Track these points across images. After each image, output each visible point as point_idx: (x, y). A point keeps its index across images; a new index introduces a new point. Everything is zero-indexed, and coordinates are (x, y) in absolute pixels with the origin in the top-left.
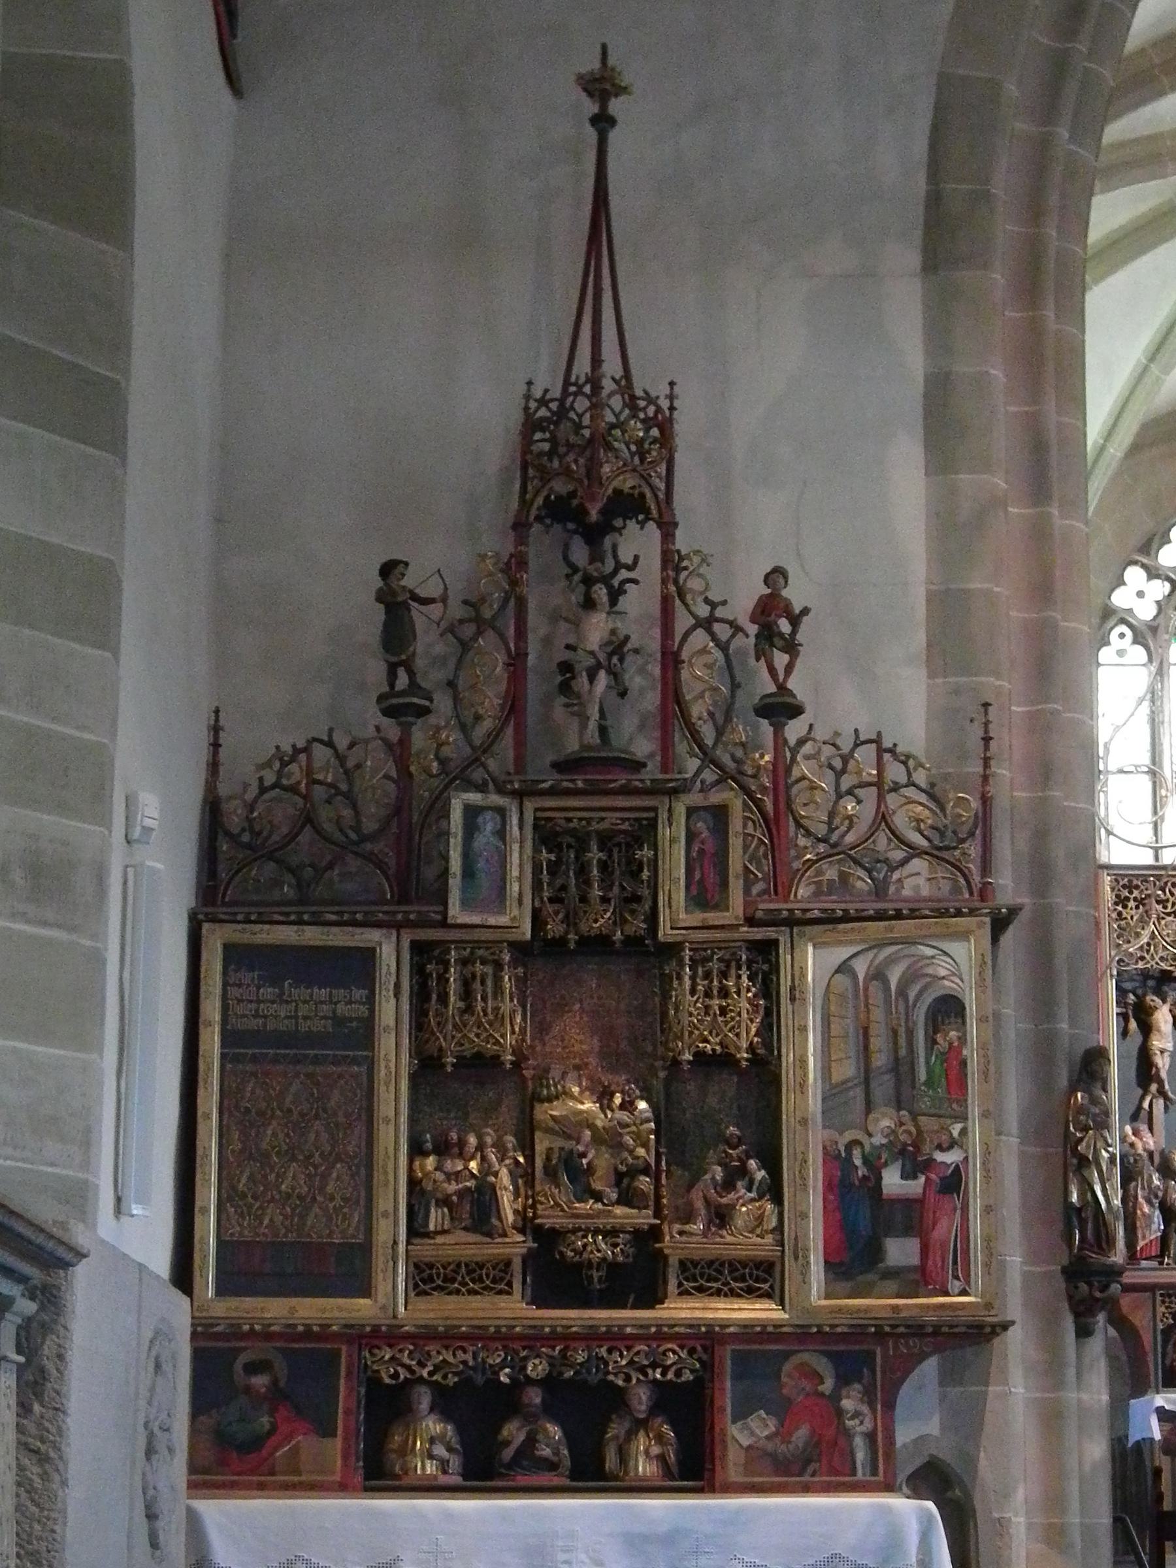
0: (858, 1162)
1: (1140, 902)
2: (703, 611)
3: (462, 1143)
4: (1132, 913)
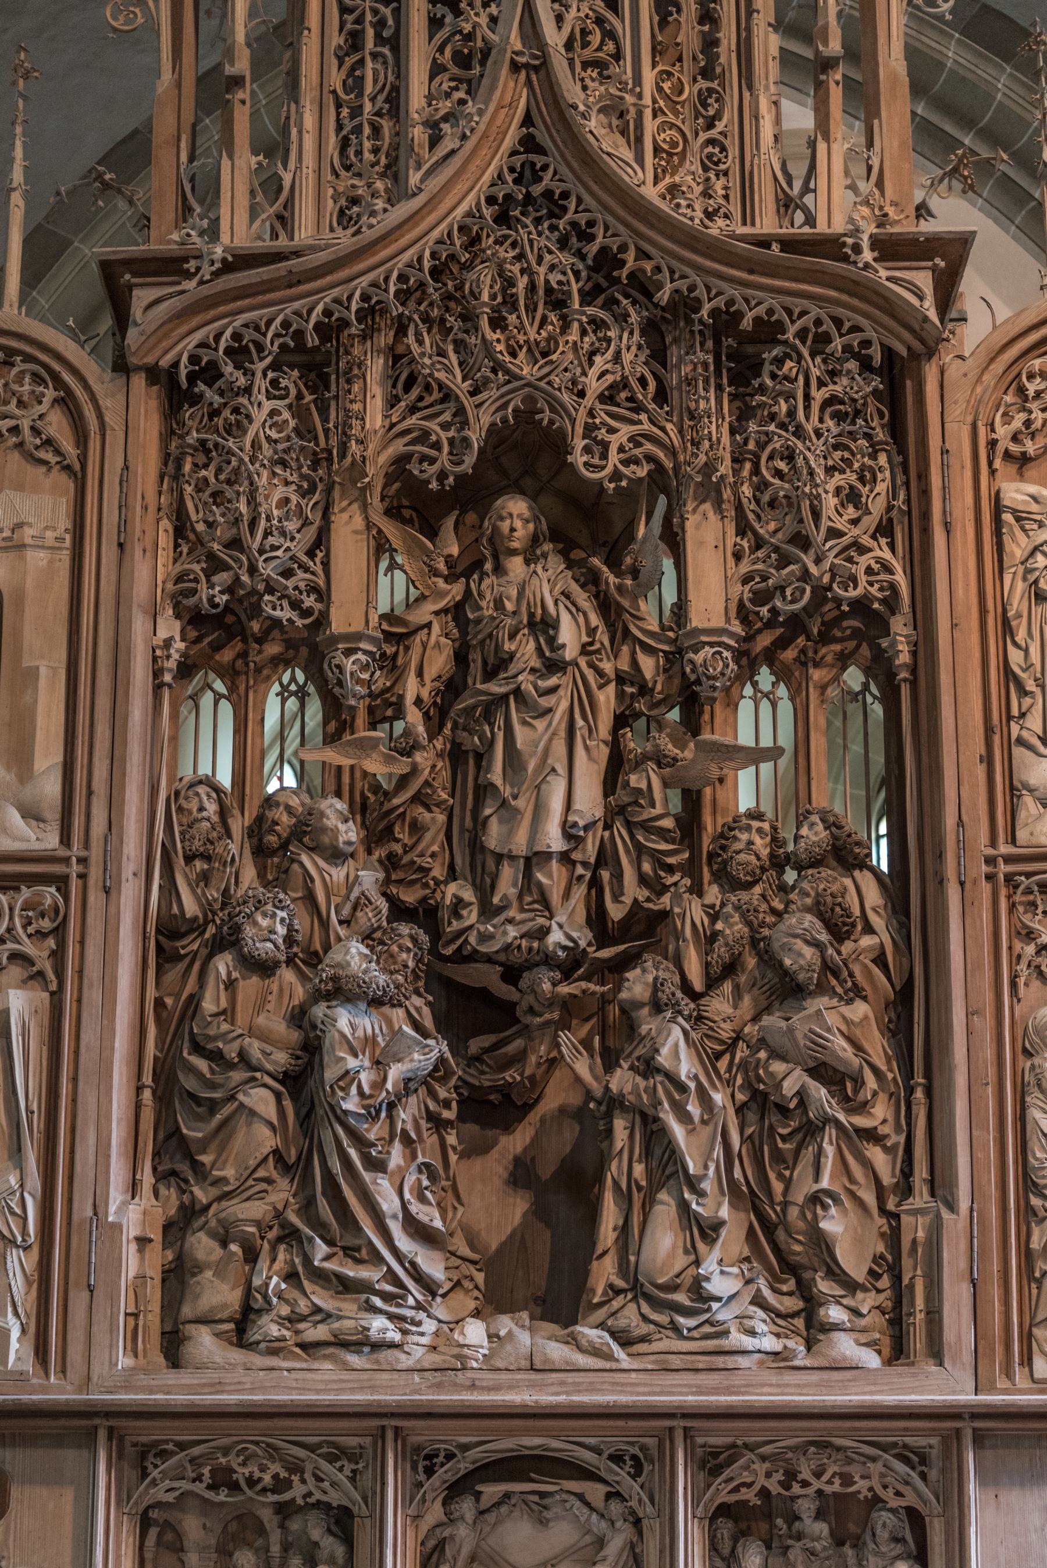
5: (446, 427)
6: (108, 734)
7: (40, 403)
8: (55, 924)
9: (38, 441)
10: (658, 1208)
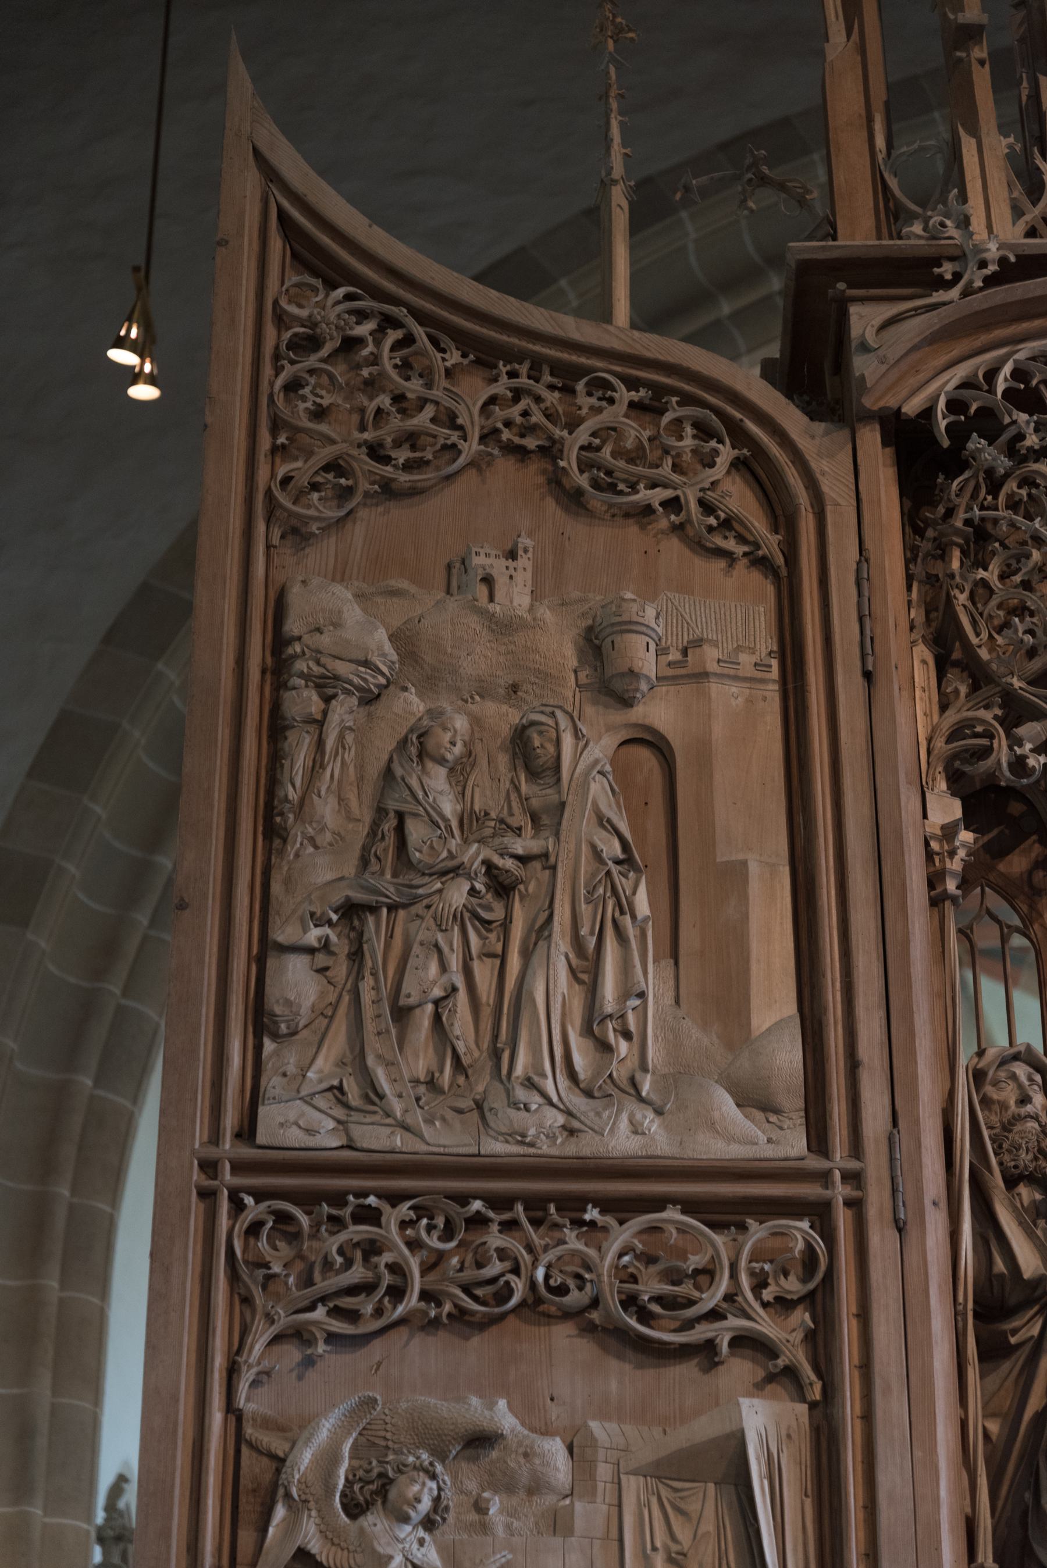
6: (877, 969)
7: (712, 465)
8: (811, 1286)
9: (712, 521)
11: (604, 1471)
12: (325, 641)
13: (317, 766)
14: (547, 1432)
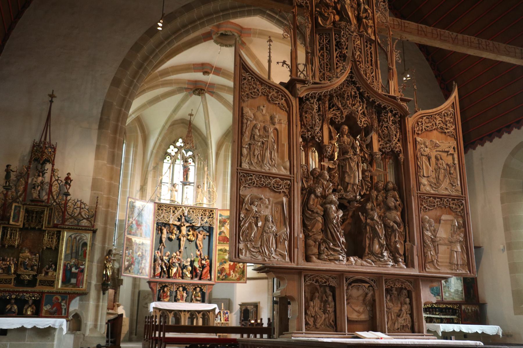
0: (69, 266)
1: (162, 210)
2: (57, 178)
3: (7, 259)
4: (160, 212)
5: (339, 114)
10: (375, 241)
11: (271, 203)
12: (247, 114)
13: (246, 128)
14: (266, 198)
